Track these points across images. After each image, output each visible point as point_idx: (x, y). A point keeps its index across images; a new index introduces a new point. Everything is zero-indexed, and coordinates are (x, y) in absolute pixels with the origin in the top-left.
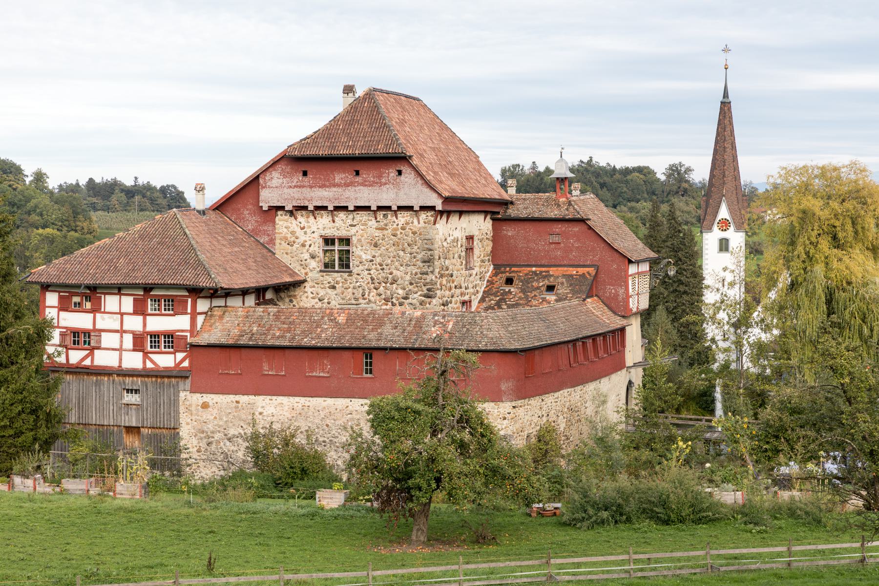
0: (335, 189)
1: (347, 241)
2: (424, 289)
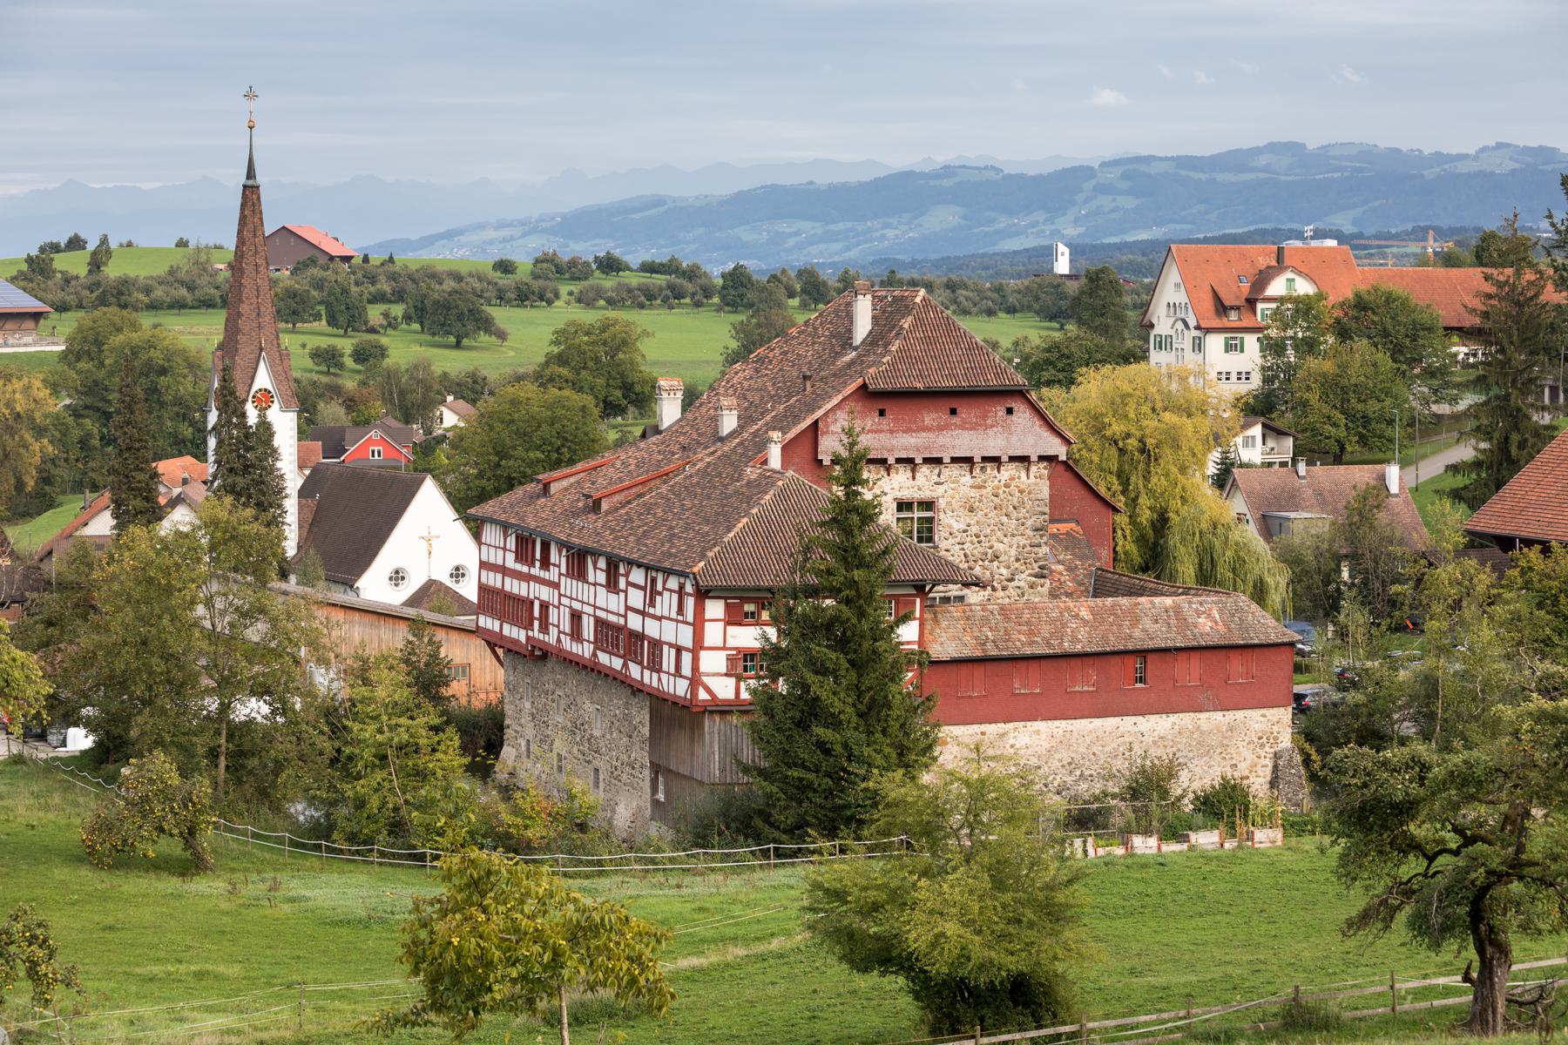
0: (924, 434)
1: (928, 505)
2: (1035, 566)
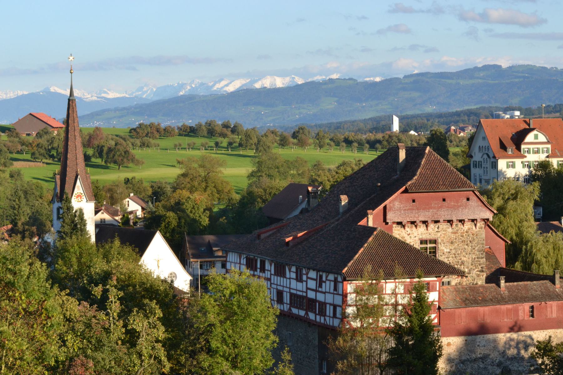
1: (435, 242)
2: (480, 267)
